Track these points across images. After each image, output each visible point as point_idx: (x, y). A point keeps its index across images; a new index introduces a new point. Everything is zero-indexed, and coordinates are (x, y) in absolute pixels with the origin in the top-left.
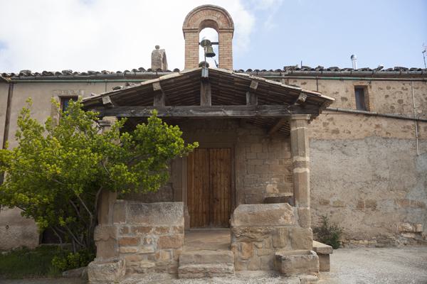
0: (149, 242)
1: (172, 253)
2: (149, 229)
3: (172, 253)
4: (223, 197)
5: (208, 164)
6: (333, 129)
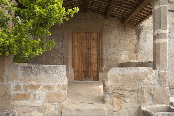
0: (37, 97)
1: (56, 105)
3: (56, 105)
4: (94, 62)
5: (85, 42)
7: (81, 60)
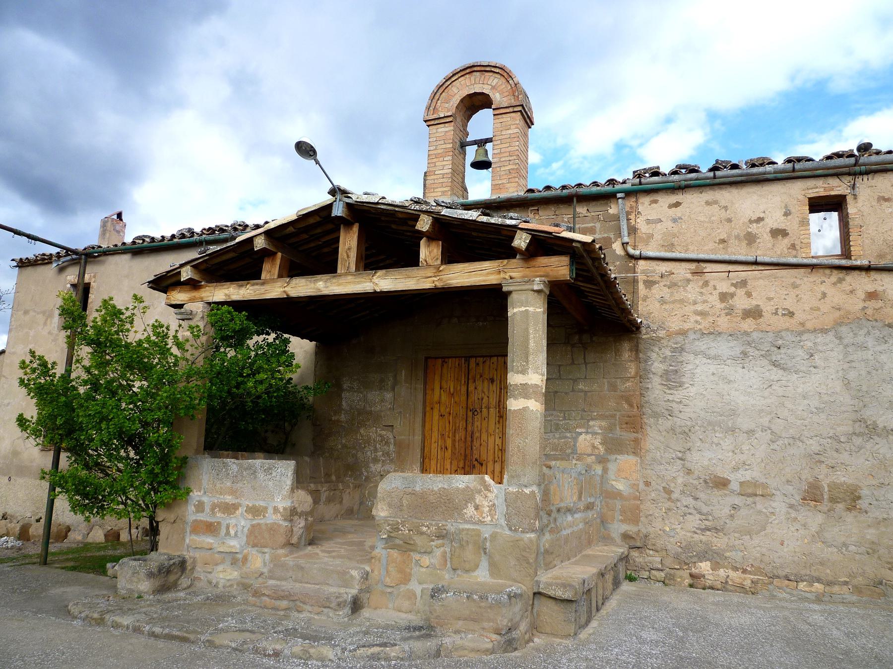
0: (232, 532)
1: (267, 556)
2: (235, 507)
4: (491, 458)
5: (464, 389)
6: (747, 307)
7: (450, 450)
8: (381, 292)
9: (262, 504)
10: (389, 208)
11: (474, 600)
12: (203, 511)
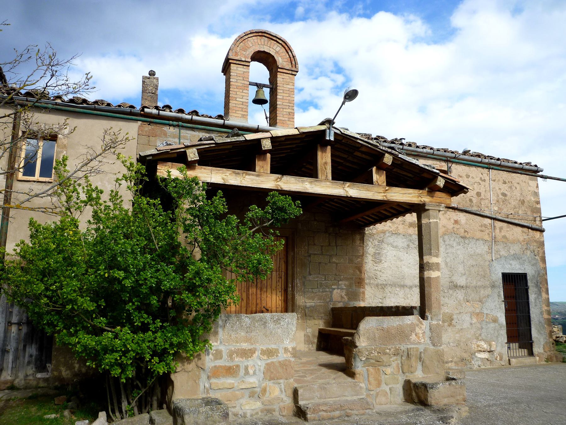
0: (251, 372)
1: (282, 385)
2: (252, 352)
3: (282, 385)
6: (411, 221)
7: (245, 301)
8: (351, 197)
9: (274, 346)
10: (364, 143)
11: (453, 385)
12: (221, 358)
